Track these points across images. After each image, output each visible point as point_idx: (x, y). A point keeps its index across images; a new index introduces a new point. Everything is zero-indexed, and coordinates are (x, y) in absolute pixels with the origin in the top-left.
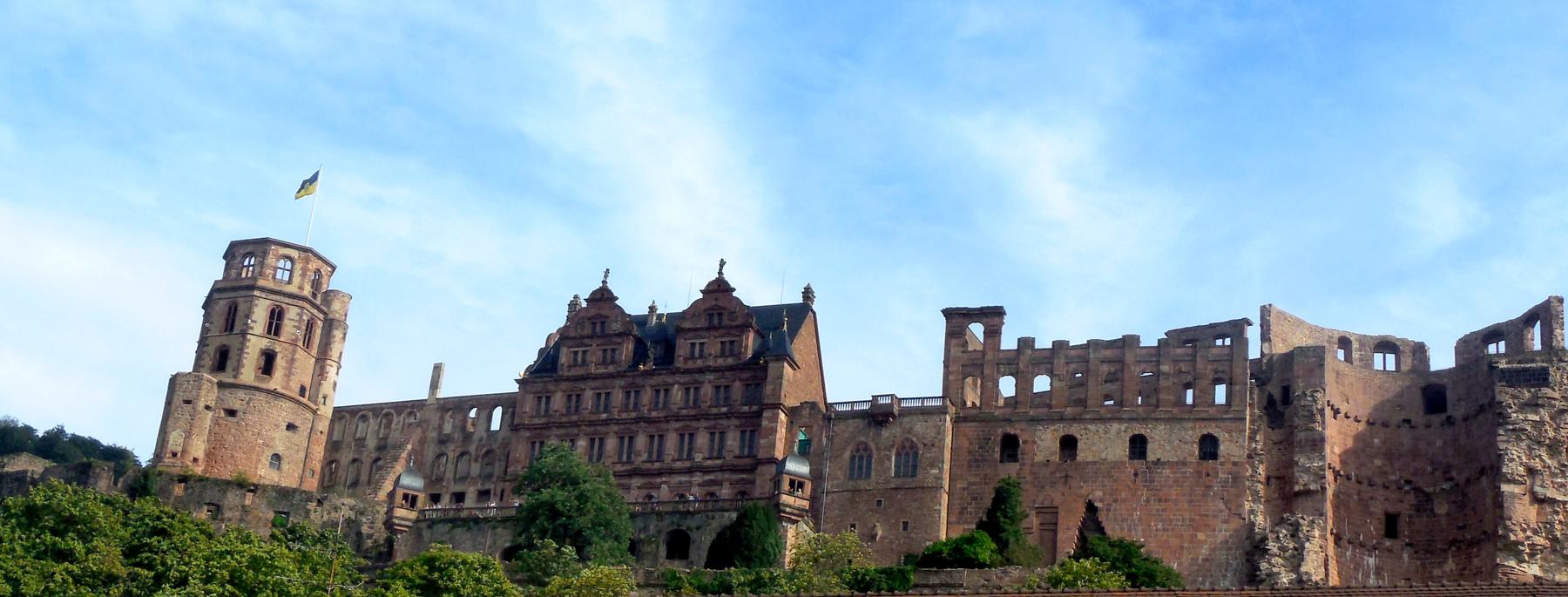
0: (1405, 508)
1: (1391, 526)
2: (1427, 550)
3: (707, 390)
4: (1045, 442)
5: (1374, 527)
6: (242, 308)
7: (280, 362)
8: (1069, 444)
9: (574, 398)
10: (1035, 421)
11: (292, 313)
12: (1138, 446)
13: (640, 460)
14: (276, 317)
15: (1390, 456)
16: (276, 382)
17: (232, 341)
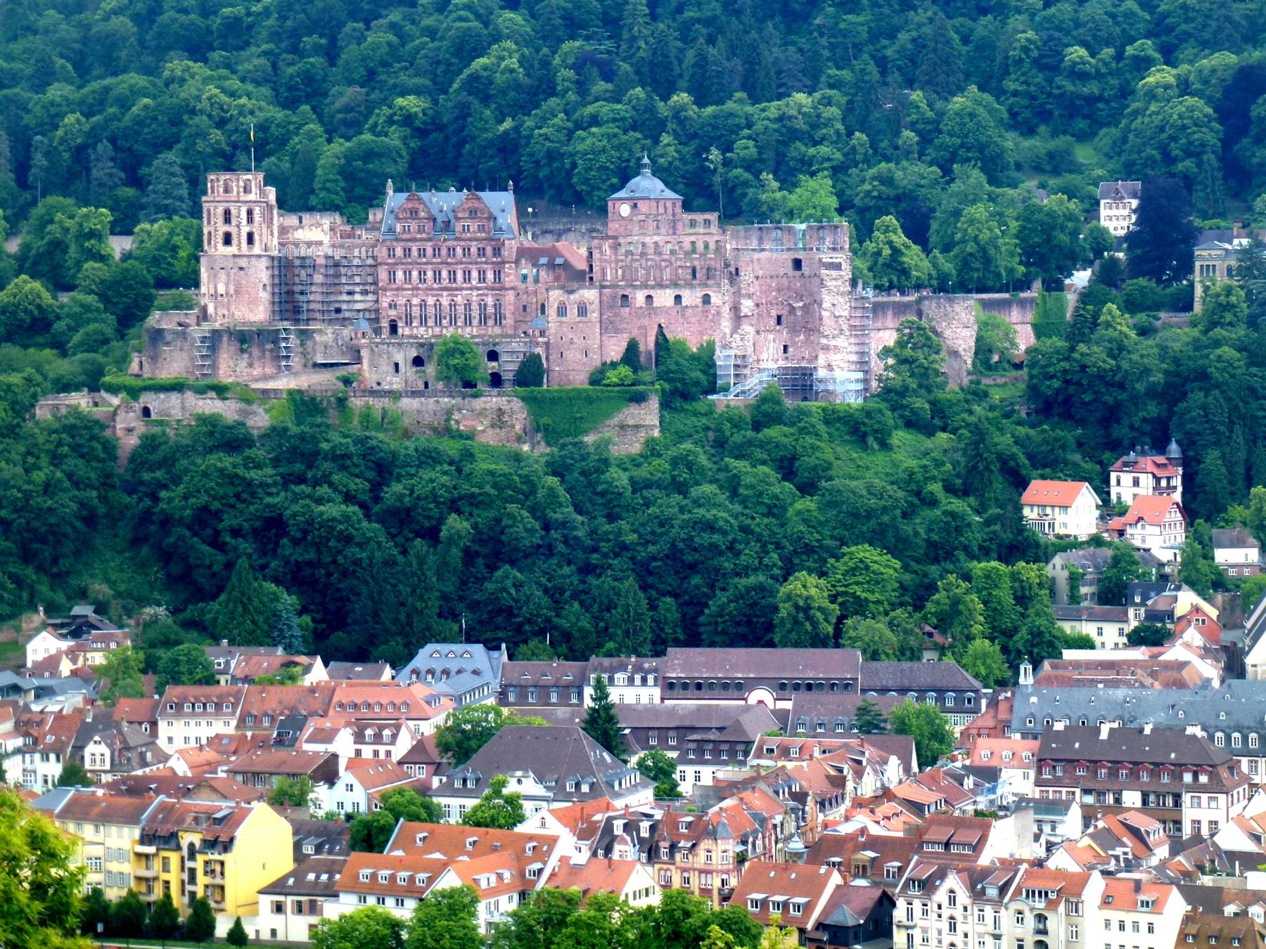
0: (784, 313)
1: (779, 320)
2: (794, 331)
3: (474, 250)
4: (640, 297)
5: (773, 321)
6: (234, 212)
7: (256, 237)
8: (649, 297)
9: (407, 252)
10: (634, 287)
11: (257, 211)
12: (678, 298)
13: (445, 283)
14: (250, 213)
15: (779, 290)
16: (257, 250)
17: (232, 229)
